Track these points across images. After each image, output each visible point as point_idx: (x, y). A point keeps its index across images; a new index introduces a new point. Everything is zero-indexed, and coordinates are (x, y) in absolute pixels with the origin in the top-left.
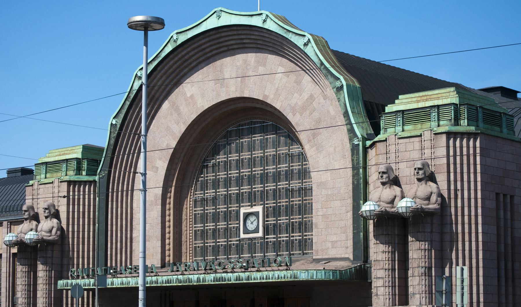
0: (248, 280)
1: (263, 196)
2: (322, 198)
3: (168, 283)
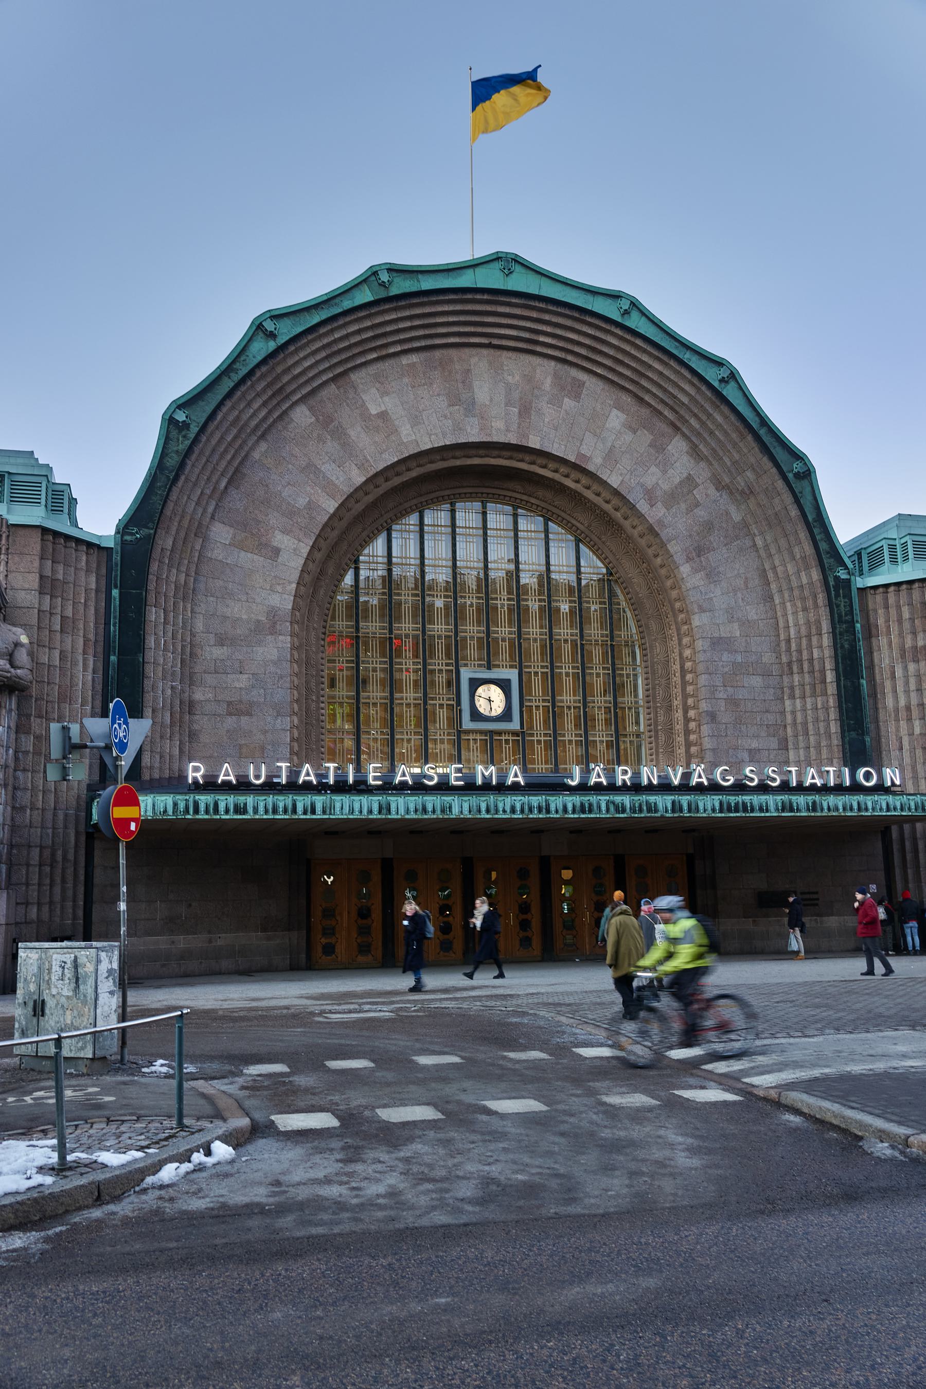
0: (814, 810)
2: (723, 666)
3: (583, 811)
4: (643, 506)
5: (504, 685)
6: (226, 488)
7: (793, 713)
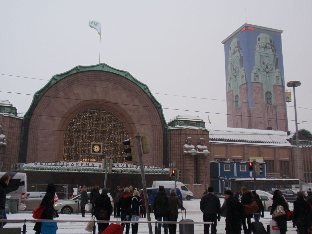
1: (103, 140)
4: (129, 112)
5: (100, 146)
6: (46, 108)
7: (156, 153)
